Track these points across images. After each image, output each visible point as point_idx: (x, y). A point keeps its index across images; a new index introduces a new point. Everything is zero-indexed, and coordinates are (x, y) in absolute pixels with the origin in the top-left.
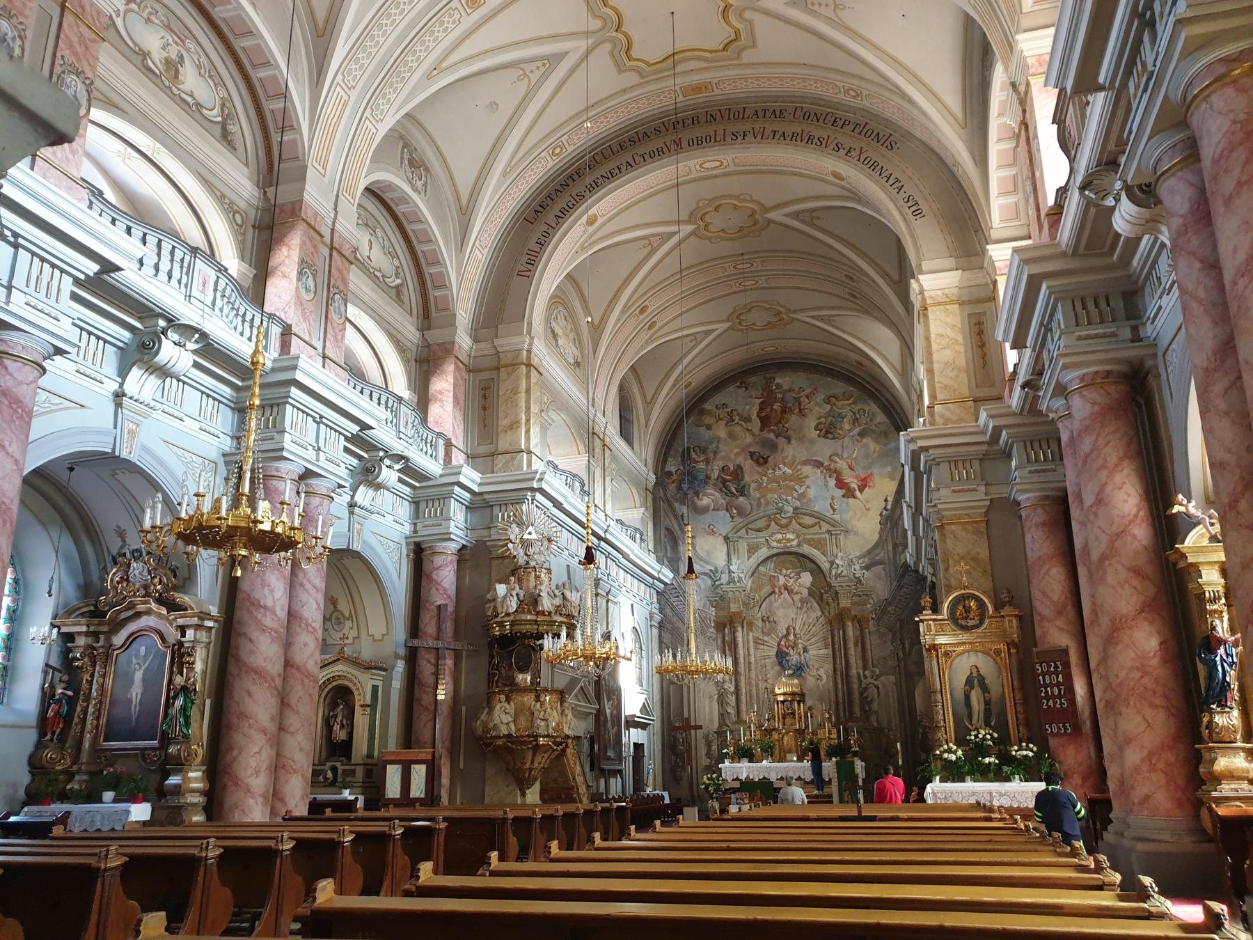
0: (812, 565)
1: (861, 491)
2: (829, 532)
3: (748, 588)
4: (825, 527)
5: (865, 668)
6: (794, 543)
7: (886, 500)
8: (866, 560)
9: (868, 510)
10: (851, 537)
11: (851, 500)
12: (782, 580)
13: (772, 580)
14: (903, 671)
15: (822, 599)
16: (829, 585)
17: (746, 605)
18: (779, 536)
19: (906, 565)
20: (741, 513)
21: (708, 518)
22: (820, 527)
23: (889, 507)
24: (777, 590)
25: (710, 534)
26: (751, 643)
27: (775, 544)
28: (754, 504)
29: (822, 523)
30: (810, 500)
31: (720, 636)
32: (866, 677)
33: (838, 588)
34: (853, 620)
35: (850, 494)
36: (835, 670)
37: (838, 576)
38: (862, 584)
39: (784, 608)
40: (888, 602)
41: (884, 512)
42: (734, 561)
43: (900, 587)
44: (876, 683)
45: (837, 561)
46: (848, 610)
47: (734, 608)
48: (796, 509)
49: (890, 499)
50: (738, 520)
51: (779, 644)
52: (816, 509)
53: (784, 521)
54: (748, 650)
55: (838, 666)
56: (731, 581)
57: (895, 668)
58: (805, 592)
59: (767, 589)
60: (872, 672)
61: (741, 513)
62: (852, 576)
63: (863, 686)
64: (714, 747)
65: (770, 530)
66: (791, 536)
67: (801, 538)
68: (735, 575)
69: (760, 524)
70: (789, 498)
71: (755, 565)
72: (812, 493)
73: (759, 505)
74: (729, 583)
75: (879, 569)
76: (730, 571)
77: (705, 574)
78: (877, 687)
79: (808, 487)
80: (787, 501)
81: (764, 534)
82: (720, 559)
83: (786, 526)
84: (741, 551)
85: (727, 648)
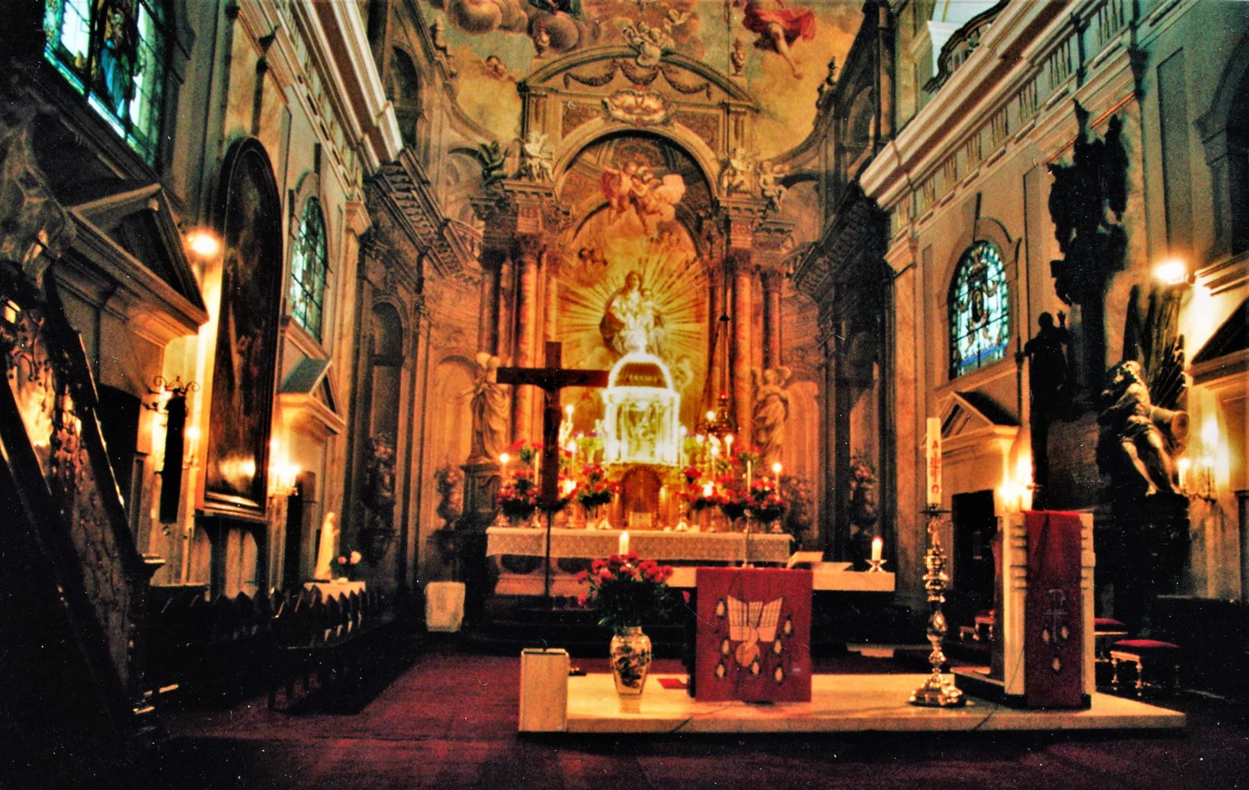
0: (686, 163)
1: (790, 39)
2: (725, 106)
3: (558, 191)
4: (718, 95)
5: (767, 363)
6: (658, 117)
7: (831, 66)
8: (787, 168)
9: (799, 77)
10: (764, 122)
11: (770, 55)
12: (627, 184)
13: (607, 182)
14: (833, 374)
15: (699, 228)
16: (715, 204)
17: (551, 222)
18: (630, 100)
19: (855, 189)
20: (557, 42)
21: (485, 43)
22: (709, 95)
23: (835, 78)
24: (615, 202)
25: (489, 74)
26: (554, 299)
27: (619, 113)
28: (587, 30)
29: (714, 88)
30: (695, 41)
31: (489, 278)
32: (766, 382)
33: (732, 213)
34: (753, 274)
35: (768, 42)
36: (711, 363)
37: (732, 190)
38: (776, 211)
39: (625, 235)
40: (819, 249)
41: (826, 87)
42: (534, 134)
43: (840, 225)
44: (784, 394)
45: (735, 163)
46: (745, 255)
47: (524, 226)
48: (666, 53)
49: (840, 65)
50: (551, 56)
51: (609, 305)
52: (705, 60)
53: (641, 73)
54: (546, 311)
55: (718, 357)
56: (524, 172)
57: (819, 369)
58: (669, 213)
59: (597, 197)
60: (780, 373)
61: (557, 42)
62: (758, 194)
63: (760, 397)
64: (458, 496)
65: (614, 84)
66: (652, 103)
67: (672, 110)
68: (534, 162)
69: (587, 71)
70: (656, 31)
71: (576, 149)
72: (701, 28)
73: (595, 34)
74: (519, 176)
75: (806, 187)
76: (524, 154)
77: (472, 152)
78: (785, 402)
79: (694, 16)
80: (650, 34)
81: (602, 91)
82: (505, 128)
83: (646, 82)
84: (550, 117)
85: (502, 303)
